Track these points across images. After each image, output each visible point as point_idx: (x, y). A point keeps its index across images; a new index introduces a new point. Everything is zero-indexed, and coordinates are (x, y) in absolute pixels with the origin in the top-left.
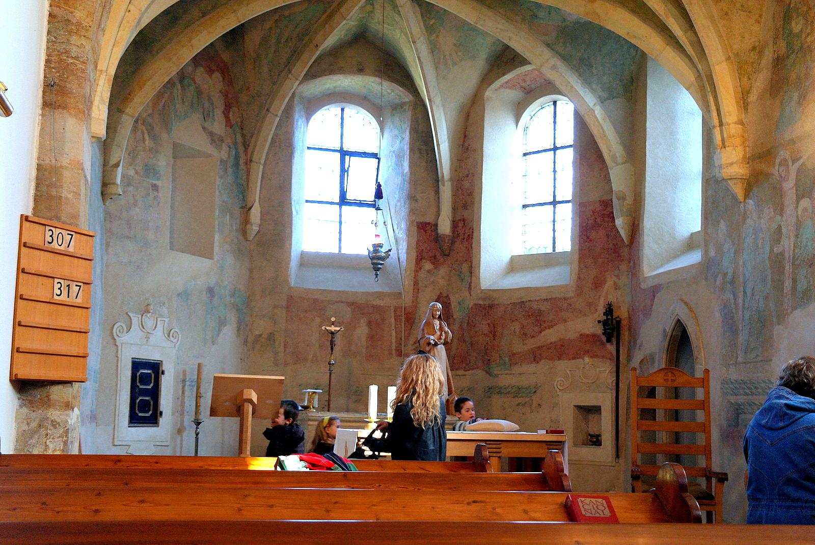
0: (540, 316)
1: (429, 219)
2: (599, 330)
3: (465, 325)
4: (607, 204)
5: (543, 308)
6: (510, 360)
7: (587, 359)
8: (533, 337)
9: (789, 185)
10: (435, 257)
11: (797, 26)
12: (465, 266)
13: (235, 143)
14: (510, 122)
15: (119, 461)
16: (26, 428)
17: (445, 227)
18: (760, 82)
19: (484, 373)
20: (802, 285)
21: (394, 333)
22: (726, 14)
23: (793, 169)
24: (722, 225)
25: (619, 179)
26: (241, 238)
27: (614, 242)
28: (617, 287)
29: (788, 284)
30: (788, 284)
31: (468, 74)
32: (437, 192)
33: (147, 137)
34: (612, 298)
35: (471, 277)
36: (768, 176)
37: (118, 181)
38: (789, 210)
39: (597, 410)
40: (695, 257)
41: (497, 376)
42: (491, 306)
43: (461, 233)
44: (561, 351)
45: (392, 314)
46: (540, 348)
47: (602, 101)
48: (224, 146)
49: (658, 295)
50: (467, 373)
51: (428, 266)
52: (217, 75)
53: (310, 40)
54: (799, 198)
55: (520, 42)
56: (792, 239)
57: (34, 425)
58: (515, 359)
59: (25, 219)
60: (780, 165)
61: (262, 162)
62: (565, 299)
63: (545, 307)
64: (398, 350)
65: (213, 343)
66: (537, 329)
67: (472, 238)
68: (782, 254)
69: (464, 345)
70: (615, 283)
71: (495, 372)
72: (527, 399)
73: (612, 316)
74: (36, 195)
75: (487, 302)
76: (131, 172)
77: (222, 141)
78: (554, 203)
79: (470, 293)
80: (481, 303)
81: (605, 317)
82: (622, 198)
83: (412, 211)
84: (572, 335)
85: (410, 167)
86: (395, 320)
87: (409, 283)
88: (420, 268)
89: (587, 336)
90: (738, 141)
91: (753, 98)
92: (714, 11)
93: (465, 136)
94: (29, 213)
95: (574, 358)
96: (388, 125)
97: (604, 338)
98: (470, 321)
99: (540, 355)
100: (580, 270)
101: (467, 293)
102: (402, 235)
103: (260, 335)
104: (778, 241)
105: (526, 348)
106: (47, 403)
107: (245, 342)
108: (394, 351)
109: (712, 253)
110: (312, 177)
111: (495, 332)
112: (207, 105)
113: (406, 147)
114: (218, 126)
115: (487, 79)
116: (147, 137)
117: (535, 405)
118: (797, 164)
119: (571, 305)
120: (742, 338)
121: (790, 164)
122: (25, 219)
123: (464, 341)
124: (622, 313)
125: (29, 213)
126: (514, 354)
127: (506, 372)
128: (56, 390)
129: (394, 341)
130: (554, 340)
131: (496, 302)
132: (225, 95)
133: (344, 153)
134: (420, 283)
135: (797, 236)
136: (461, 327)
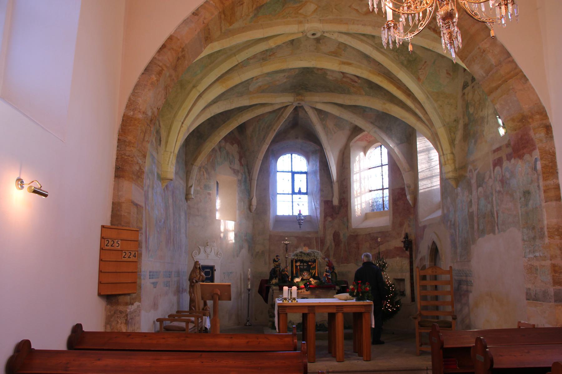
1: (329, 199)
2: (402, 245)
4: (403, 189)
7: (398, 258)
9: (473, 181)
10: (332, 215)
11: (471, 110)
12: (345, 218)
13: (245, 173)
14: (362, 154)
15: (130, 335)
16: (109, 314)
17: (336, 202)
18: (459, 134)
20: (481, 227)
22: (441, 106)
23: (475, 174)
24: (449, 199)
25: (407, 179)
26: (249, 212)
28: (409, 226)
31: (341, 138)
32: (332, 187)
33: (205, 173)
34: (408, 231)
36: (465, 177)
37: (192, 192)
38: (474, 193)
39: (403, 280)
40: (439, 213)
42: (357, 236)
47: (397, 145)
48: (240, 174)
49: (425, 230)
51: (329, 219)
52: (236, 145)
53: (272, 128)
55: (359, 122)
57: (112, 312)
59: (103, 227)
61: (256, 179)
62: (387, 232)
65: (237, 256)
68: (472, 212)
74: (112, 215)
76: (199, 188)
77: (238, 171)
78: (383, 189)
82: (409, 187)
83: (322, 196)
85: (320, 177)
87: (321, 227)
89: (398, 248)
90: (451, 162)
91: (457, 142)
92: (436, 105)
93: (343, 163)
94: (108, 224)
95: (393, 258)
96: (311, 159)
97: (405, 249)
100: (393, 218)
102: (318, 206)
104: (471, 206)
106: (118, 303)
107: (252, 255)
109: (445, 211)
110: (282, 183)
112: (231, 158)
113: (318, 169)
114: (237, 166)
115: (350, 138)
116: (205, 173)
118: (477, 171)
120: (459, 250)
122: (103, 227)
124: (412, 237)
125: (108, 224)
128: (121, 299)
132: (239, 153)
133: (293, 173)
135: (478, 204)
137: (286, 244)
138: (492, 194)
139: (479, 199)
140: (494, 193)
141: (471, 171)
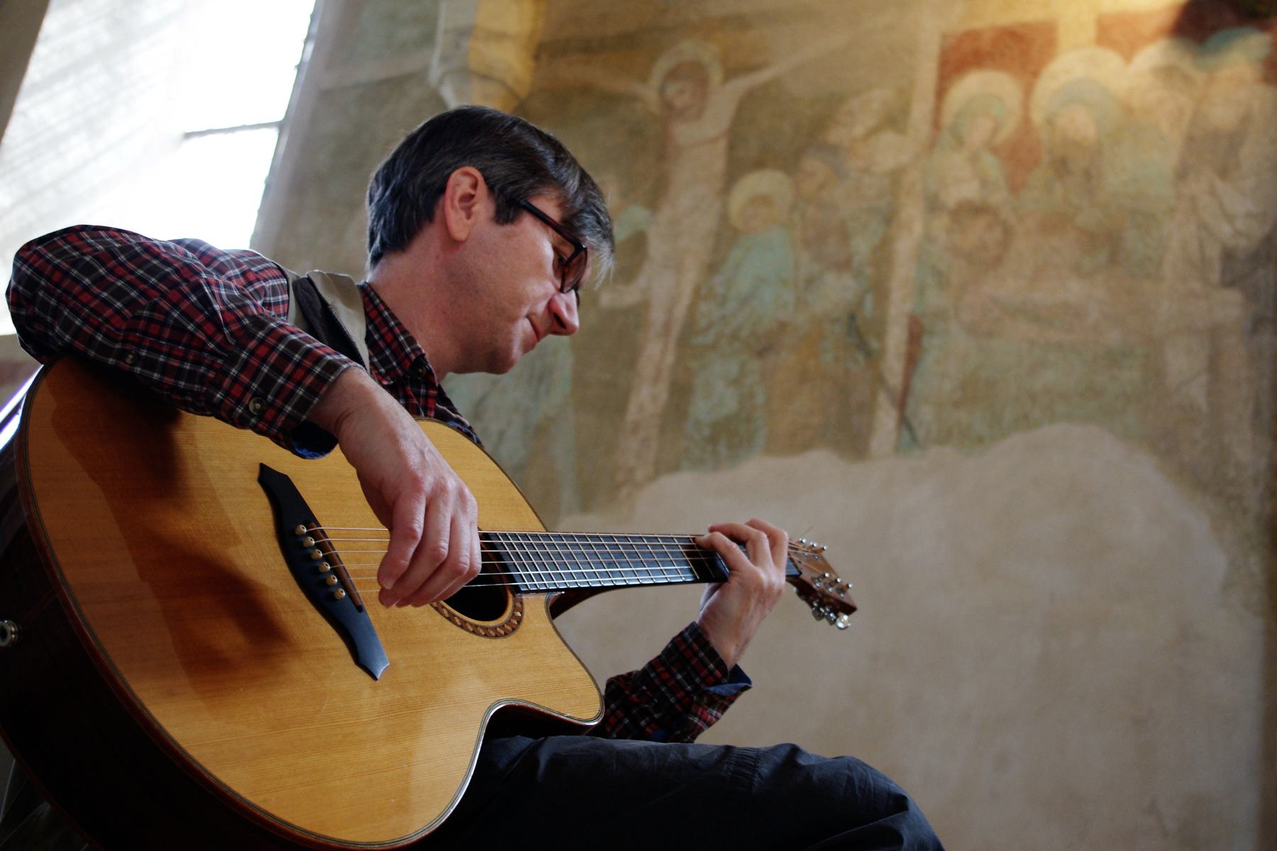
29: (647, 398)
30: (647, 398)
54: (735, 169)
56: (691, 277)
60: (673, 75)
68: (637, 315)
121: (716, 75)
135: (712, 268)
138: (890, 218)
139: (726, 236)
140: (912, 212)
141: (695, 74)
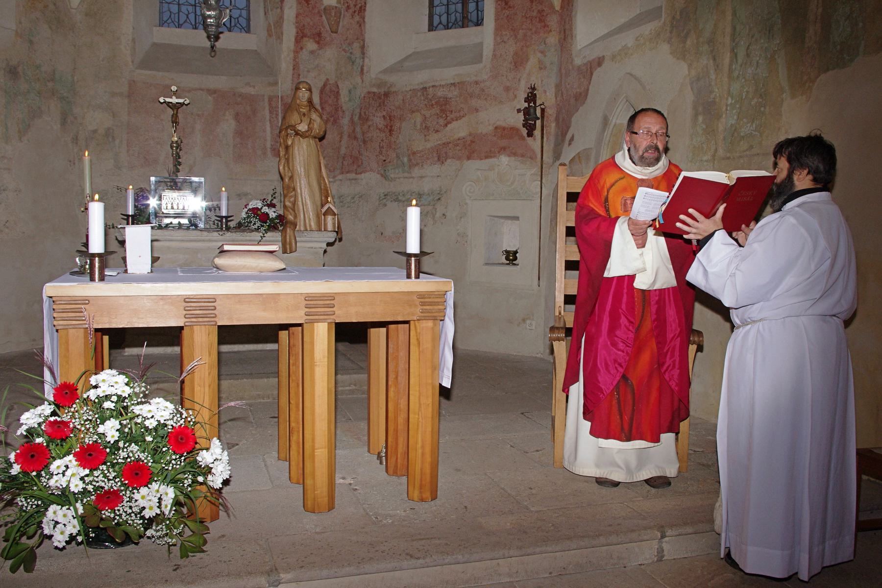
0: (446, 105)
3: (356, 118)
5: (450, 96)
6: (410, 160)
7: (504, 159)
8: (437, 131)
10: (319, 35)
19: (379, 176)
21: (268, 129)
27: (540, 7)
28: (542, 67)
34: (534, 80)
35: (363, 58)
41: (394, 179)
42: (386, 95)
43: (352, 6)
44: (472, 148)
45: (267, 105)
46: (446, 144)
50: (358, 176)
51: (311, 45)
58: (415, 160)
62: (477, 83)
63: (454, 93)
64: (274, 150)
66: (442, 121)
67: (365, 10)
69: (355, 143)
70: (540, 62)
71: (392, 176)
72: (430, 208)
73: (535, 103)
75: (382, 91)
79: (362, 78)
80: (375, 90)
81: (526, 105)
84: (486, 129)
86: (270, 112)
88: (302, 48)
89: (504, 129)
95: (486, 157)
97: (524, 132)
98: (363, 114)
99: (446, 153)
101: (359, 80)
103: (95, 131)
105: (429, 145)
108: (269, 150)
111: (391, 126)
117: (438, 215)
119: (483, 90)
123: (355, 138)
124: (547, 98)
126: (414, 153)
127: (406, 175)
129: (269, 138)
130: (463, 134)
131: (393, 89)
134: (301, 67)
136: (352, 121)
137: (176, 107)
